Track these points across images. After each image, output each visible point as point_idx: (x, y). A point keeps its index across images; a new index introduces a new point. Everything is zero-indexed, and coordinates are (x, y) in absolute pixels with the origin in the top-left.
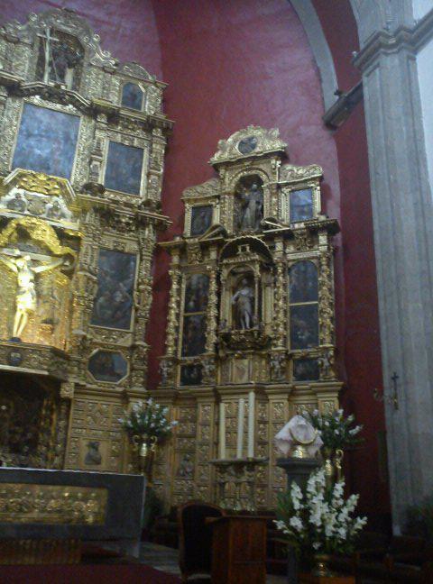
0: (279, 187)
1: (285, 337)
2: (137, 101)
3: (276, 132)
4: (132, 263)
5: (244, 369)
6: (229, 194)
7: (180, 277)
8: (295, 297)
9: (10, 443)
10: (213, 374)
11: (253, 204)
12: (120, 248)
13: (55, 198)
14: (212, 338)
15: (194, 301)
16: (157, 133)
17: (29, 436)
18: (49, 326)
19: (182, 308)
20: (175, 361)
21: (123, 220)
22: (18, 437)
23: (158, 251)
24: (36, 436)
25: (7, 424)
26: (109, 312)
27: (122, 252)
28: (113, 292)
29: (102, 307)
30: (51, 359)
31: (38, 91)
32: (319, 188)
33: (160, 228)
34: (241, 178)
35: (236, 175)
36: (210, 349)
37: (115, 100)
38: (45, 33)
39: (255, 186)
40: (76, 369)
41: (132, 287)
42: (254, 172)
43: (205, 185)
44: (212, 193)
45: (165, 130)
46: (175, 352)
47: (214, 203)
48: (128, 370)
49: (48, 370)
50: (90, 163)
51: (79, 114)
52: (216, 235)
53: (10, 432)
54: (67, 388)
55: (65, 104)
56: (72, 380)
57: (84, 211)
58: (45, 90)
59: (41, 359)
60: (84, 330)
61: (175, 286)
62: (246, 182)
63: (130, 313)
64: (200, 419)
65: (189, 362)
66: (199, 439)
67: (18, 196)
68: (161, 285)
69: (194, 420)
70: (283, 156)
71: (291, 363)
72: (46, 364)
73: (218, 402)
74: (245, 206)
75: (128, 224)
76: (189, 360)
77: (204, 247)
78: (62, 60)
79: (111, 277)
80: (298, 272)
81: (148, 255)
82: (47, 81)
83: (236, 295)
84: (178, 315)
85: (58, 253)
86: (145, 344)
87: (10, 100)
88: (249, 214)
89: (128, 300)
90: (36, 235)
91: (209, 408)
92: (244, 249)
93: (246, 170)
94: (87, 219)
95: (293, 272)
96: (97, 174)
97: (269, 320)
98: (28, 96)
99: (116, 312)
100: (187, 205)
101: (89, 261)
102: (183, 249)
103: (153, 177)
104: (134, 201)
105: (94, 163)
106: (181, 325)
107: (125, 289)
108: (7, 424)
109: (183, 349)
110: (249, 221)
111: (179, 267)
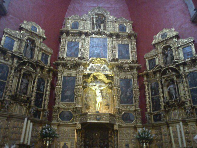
0: (178, 48)
1: (190, 101)
2: (124, 29)
3: (173, 29)
4: (131, 82)
5: (176, 114)
6: (160, 53)
7: (148, 85)
8: (191, 85)
9: (100, 146)
10: (165, 117)
11: (169, 55)
12: (126, 78)
13: (103, 65)
14: (163, 104)
15: (154, 92)
16: (132, 38)
17: (106, 143)
18: (107, 106)
19: (150, 95)
20: (151, 114)
21: (126, 68)
22: (102, 144)
23: (139, 77)
24: (108, 143)
25: (98, 140)
26: (126, 99)
27: (127, 79)
28: (126, 92)
29: (123, 98)
30: (109, 117)
31: (93, 33)
32: (193, 45)
33: (138, 69)
34: (164, 47)
35: (162, 47)
36: (163, 108)
37: (117, 30)
38: (93, 15)
39: (169, 49)
40: (118, 120)
41: (132, 90)
42: (168, 44)
43: (151, 52)
44: (154, 54)
45: (135, 37)
46: (150, 110)
47: (155, 57)
48: (135, 118)
49: (109, 121)
50: (113, 52)
51: (107, 37)
52: (158, 68)
53: (100, 142)
54: (116, 126)
55: (102, 35)
56: (117, 123)
57: (113, 68)
59: (106, 117)
60: (118, 106)
61: (146, 88)
62: (165, 48)
63: (133, 99)
64: (163, 133)
65: (156, 113)
66: (164, 141)
67: (92, 66)
68: (142, 88)
69: (161, 134)
70: (178, 37)
71: (194, 109)
72: (108, 119)
73: (168, 127)
74: (167, 56)
75: (127, 69)
76: (156, 112)
77: (155, 73)
78: (99, 22)
79: (125, 87)
80: (191, 76)
81: (136, 79)
82: (96, 30)
83: (169, 88)
84: (149, 98)
85: (107, 82)
86: (139, 109)
87: (86, 38)
88: (168, 59)
89: (131, 95)
90: (99, 78)
91: (166, 129)
92: (169, 71)
93: (165, 44)
94: (114, 70)
95: (189, 77)
96: (115, 55)
97: (182, 95)
98: (91, 35)
99: (128, 99)
100: (146, 60)
101: (117, 83)
102: (147, 75)
103: (133, 53)
104: (128, 62)
105: (114, 52)
106: (151, 101)
107: (130, 91)
108: (98, 140)
109: (153, 109)
110: (169, 61)
111: (147, 81)
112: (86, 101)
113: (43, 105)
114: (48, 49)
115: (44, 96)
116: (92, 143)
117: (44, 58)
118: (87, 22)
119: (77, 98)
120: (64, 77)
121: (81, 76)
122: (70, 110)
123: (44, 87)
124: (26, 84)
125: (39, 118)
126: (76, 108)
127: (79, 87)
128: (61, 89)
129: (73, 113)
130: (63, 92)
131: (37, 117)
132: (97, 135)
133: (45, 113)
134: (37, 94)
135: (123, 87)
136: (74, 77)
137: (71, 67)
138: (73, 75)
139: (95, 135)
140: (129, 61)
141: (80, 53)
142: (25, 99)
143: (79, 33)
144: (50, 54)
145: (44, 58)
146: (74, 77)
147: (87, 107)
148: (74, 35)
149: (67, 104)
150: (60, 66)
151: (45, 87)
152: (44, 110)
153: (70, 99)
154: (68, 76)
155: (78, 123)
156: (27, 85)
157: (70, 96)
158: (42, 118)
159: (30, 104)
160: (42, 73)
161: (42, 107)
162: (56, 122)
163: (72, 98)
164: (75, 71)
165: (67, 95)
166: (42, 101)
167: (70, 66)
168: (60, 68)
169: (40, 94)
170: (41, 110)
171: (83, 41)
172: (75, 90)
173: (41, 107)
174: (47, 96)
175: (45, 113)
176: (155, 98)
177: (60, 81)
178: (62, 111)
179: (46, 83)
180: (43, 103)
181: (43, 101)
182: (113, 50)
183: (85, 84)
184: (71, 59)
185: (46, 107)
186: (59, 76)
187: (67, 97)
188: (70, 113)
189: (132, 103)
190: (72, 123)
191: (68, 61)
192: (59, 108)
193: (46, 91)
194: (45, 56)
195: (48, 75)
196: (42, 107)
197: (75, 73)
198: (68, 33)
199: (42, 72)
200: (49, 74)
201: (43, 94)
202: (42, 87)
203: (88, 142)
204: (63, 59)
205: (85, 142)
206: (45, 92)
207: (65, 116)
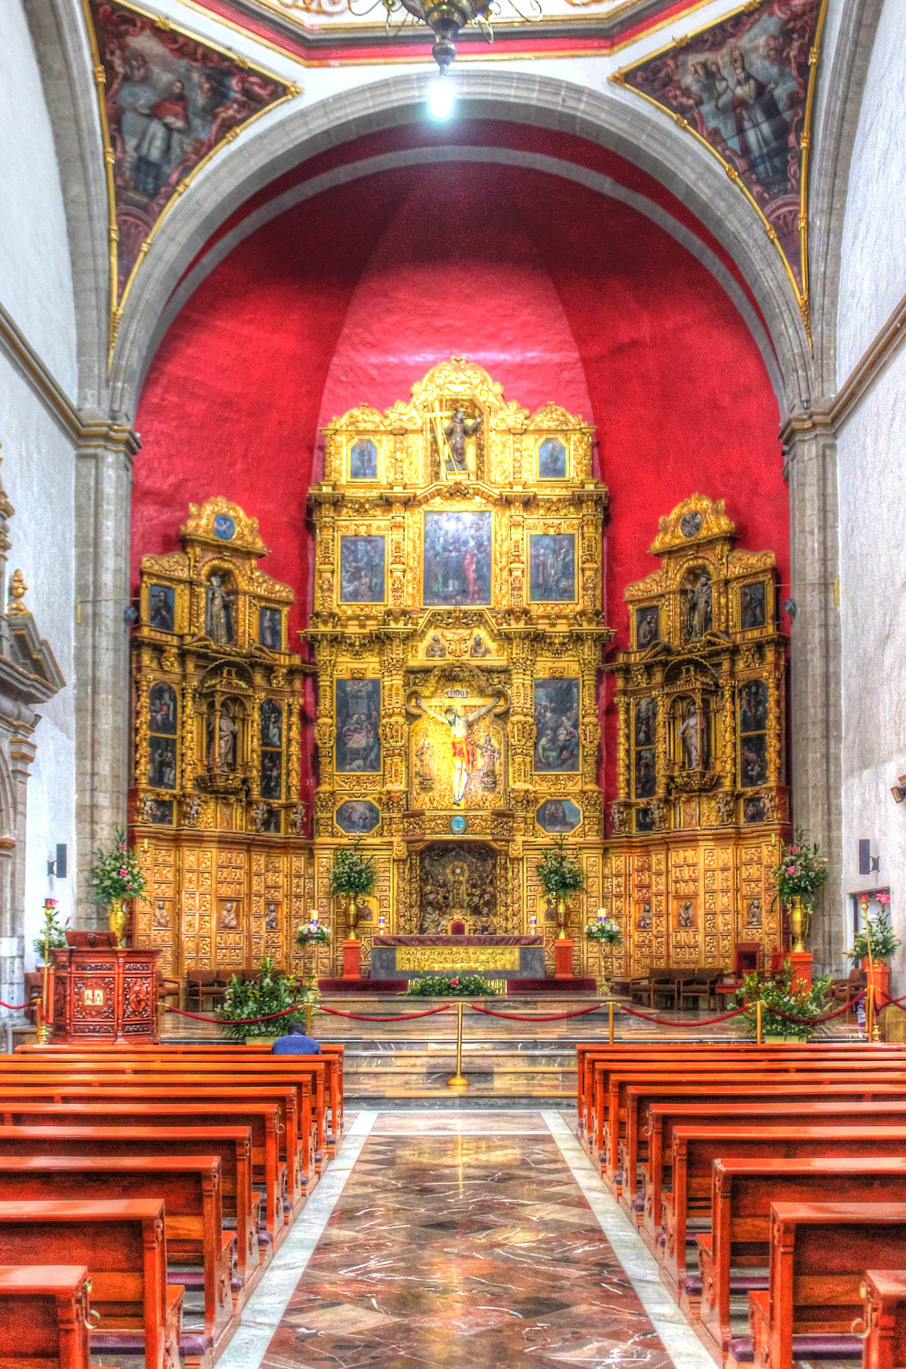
4: (575, 690)
12: (557, 675)
16: (588, 510)
17: (487, 897)
18: (490, 780)
19: (633, 741)
21: (557, 641)
22: (476, 899)
24: (494, 896)
25: (463, 888)
27: (561, 679)
46: (628, 794)
50: (510, 571)
53: (468, 895)
58: (445, 490)
61: (622, 717)
79: (553, 711)
81: (590, 680)
84: (628, 751)
89: (574, 737)
99: (561, 752)
100: (630, 607)
103: (588, 573)
105: (515, 573)
108: (463, 888)
111: (625, 693)
112: (419, 763)
113: (284, 790)
114: (277, 588)
115: (284, 759)
116: (446, 898)
117: (266, 624)
118: (411, 437)
119: (388, 760)
120: (341, 683)
121: (398, 681)
122: (368, 798)
123: (280, 729)
124: (231, 737)
125: (278, 829)
126: (389, 792)
127: (393, 720)
128: (333, 728)
129: (380, 808)
130: (341, 739)
131: (273, 825)
132: (458, 871)
133: (292, 816)
134: (264, 755)
135: (546, 708)
136: (376, 683)
137: (360, 646)
138: (370, 675)
139: (453, 872)
140: (571, 608)
141: (390, 586)
142: (237, 784)
143: (381, 498)
144: (287, 603)
145: (266, 624)
146: (376, 683)
147: (426, 784)
148: (361, 508)
149: (358, 777)
150: (325, 642)
151: (284, 727)
152: (289, 807)
153: (365, 759)
154: (354, 679)
155: (396, 840)
156: (234, 736)
157: (365, 749)
158: (286, 829)
159: (248, 792)
160: (271, 684)
161: (283, 796)
162: (329, 840)
163: (372, 756)
164: (377, 659)
165: (355, 746)
166: (279, 776)
167: (357, 643)
168: (323, 654)
169: (272, 754)
170: (282, 806)
171: (397, 535)
172: (380, 731)
173: (279, 798)
174: (294, 758)
175: (292, 816)
176: (644, 754)
177: (327, 702)
178: (342, 802)
179: (285, 714)
180: (284, 784)
181: (284, 777)
182: (513, 565)
183: (413, 702)
184: (358, 612)
185: (295, 798)
186: (324, 681)
187: (355, 753)
188: (372, 808)
189: (574, 767)
190: (377, 841)
191: (349, 619)
192: (332, 793)
193: (289, 741)
194: (272, 620)
195: (287, 689)
196: (283, 796)
197: (377, 666)
198: (337, 503)
199: (269, 681)
200: (291, 683)
201: (279, 754)
202: (273, 731)
203: (431, 893)
204: (332, 615)
205: (422, 895)
206: (284, 745)
207: (356, 817)
